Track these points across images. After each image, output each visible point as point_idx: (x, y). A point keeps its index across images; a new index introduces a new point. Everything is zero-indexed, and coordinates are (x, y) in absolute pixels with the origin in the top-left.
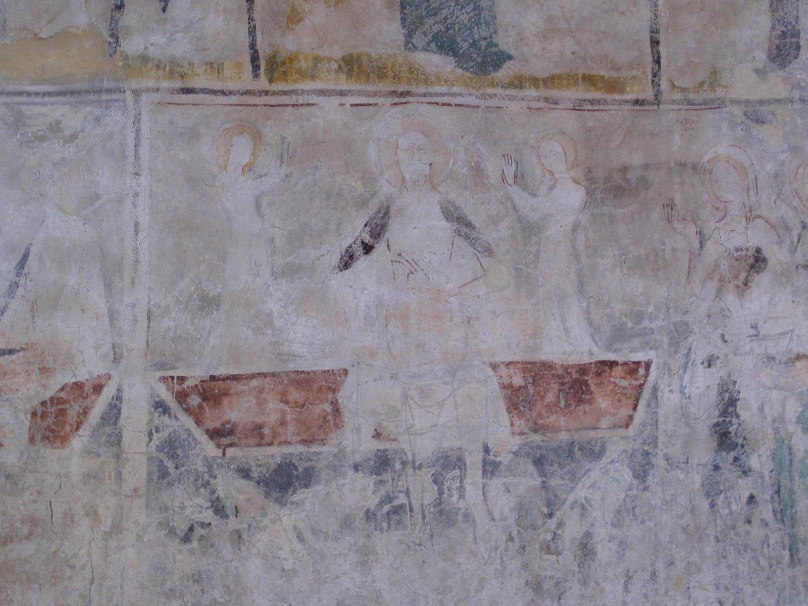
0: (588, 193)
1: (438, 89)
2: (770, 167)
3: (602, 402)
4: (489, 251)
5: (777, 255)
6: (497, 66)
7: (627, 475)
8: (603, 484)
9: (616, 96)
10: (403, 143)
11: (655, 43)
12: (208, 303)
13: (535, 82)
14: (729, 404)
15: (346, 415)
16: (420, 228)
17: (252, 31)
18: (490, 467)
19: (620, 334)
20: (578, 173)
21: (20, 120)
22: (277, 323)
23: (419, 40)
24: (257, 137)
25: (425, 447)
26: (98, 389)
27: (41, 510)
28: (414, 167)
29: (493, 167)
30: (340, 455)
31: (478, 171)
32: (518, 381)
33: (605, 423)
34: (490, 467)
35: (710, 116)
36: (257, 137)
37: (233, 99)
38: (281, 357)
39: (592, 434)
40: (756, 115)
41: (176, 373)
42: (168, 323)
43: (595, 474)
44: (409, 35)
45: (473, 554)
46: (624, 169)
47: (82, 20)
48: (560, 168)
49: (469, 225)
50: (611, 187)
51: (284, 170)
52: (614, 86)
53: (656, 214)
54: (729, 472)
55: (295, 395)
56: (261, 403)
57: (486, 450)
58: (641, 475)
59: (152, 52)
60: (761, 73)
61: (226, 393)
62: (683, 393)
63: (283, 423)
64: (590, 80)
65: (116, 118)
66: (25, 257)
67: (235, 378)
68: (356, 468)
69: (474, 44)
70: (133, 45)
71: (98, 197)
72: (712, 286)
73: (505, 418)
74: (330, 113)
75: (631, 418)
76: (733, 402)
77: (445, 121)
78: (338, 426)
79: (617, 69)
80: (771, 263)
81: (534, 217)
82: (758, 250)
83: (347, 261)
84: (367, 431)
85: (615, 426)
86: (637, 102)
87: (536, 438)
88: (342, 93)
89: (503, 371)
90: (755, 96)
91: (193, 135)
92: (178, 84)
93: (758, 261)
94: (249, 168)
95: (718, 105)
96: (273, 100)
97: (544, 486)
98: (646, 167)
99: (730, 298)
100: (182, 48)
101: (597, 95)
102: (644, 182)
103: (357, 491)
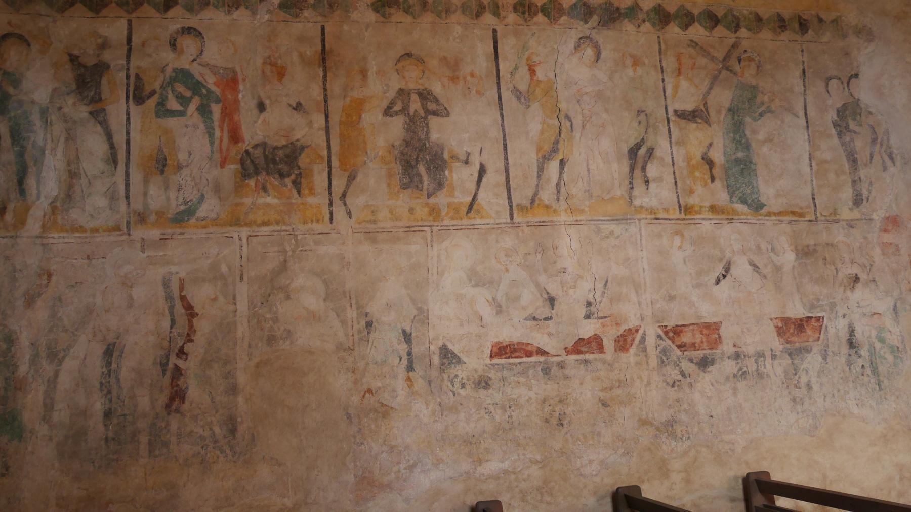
0: (797, 255)
1: (742, 217)
2: (858, 244)
3: (809, 332)
4: (765, 277)
5: (863, 277)
6: (762, 208)
7: (820, 358)
8: (812, 362)
10: (733, 237)
11: (814, 199)
12: (671, 298)
13: (775, 214)
14: (852, 332)
15: (723, 338)
16: (741, 269)
17: (678, 197)
18: (774, 357)
19: (813, 307)
20: (792, 248)
21: (599, 231)
22: (697, 305)
23: (734, 199)
24: (682, 236)
25: (751, 350)
26: (637, 331)
27: (622, 377)
28: (737, 247)
29: (763, 246)
30: (723, 353)
31: (759, 247)
32: (780, 325)
33: (811, 340)
34: (774, 357)
35: (835, 226)
36: (682, 236)
37: (673, 222)
38: (700, 317)
41: (664, 324)
42: (658, 306)
43: (809, 359)
44: (731, 198)
45: (771, 389)
46: (808, 246)
47: (619, 193)
48: (786, 246)
49: (757, 267)
50: (805, 253)
51: (693, 248)
52: (801, 215)
53: (821, 262)
54: (854, 357)
55: (705, 332)
56: (694, 335)
57: (772, 350)
58: (825, 358)
59: (644, 205)
60: (851, 209)
61: (681, 331)
62: (836, 328)
63: (702, 342)
64: (793, 213)
65: (633, 229)
66: (607, 282)
67: (684, 325)
68: (729, 358)
69: (753, 201)
70: (637, 202)
71: (629, 259)
72: (842, 289)
73: (777, 338)
74: (707, 227)
76: (853, 331)
77: (745, 228)
78: (721, 342)
79: (801, 208)
80: (861, 279)
81: (779, 264)
83: (718, 282)
84: (731, 345)
86: (810, 221)
87: (788, 346)
88: (710, 219)
89: (775, 321)
90: (850, 218)
91: (660, 236)
92: (653, 216)
93: (856, 279)
94: (680, 247)
95: (837, 221)
97: (792, 363)
98: (815, 245)
99: (849, 293)
100: (654, 203)
101: (796, 219)
102: (815, 250)
103: (730, 367)
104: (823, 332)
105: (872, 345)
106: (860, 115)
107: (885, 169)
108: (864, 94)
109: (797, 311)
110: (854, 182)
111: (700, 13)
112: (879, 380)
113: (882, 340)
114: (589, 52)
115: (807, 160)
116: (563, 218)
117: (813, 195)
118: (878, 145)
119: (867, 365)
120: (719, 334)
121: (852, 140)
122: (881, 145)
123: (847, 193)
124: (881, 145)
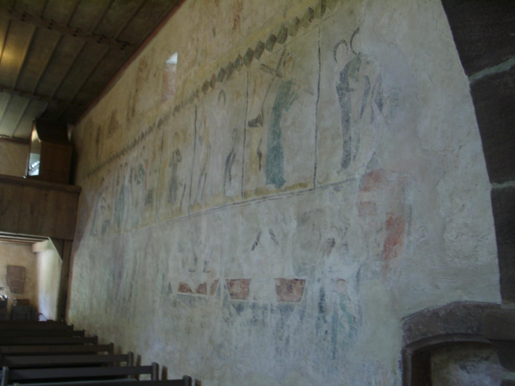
1: (271, 195)
3: (295, 292)
5: (338, 241)
8: (293, 319)
9: (306, 189)
11: (315, 168)
14: (322, 296)
16: (266, 238)
18: (272, 310)
32: (279, 284)
39: (292, 303)
40: (337, 187)
46: (305, 214)
52: (305, 185)
55: (243, 286)
58: (301, 319)
60: (338, 172)
62: (313, 290)
67: (234, 280)
75: (301, 298)
82: (334, 239)
83: (253, 248)
85: (297, 301)
86: (310, 190)
87: (281, 302)
88: (255, 200)
95: (326, 187)
96: (245, 204)
97: (282, 319)
98: (310, 212)
104: (304, 294)
105: (336, 313)
106: (358, 70)
107: (373, 118)
108: (364, 45)
109: (290, 274)
110: (345, 142)
111: (267, 41)
112: (335, 348)
113: (343, 308)
114: (222, 99)
115: (314, 133)
116: (203, 210)
117: (316, 164)
118: (370, 94)
119: (330, 331)
120: (248, 289)
121: (349, 99)
122: (373, 93)
123: (340, 155)
124: (373, 93)
